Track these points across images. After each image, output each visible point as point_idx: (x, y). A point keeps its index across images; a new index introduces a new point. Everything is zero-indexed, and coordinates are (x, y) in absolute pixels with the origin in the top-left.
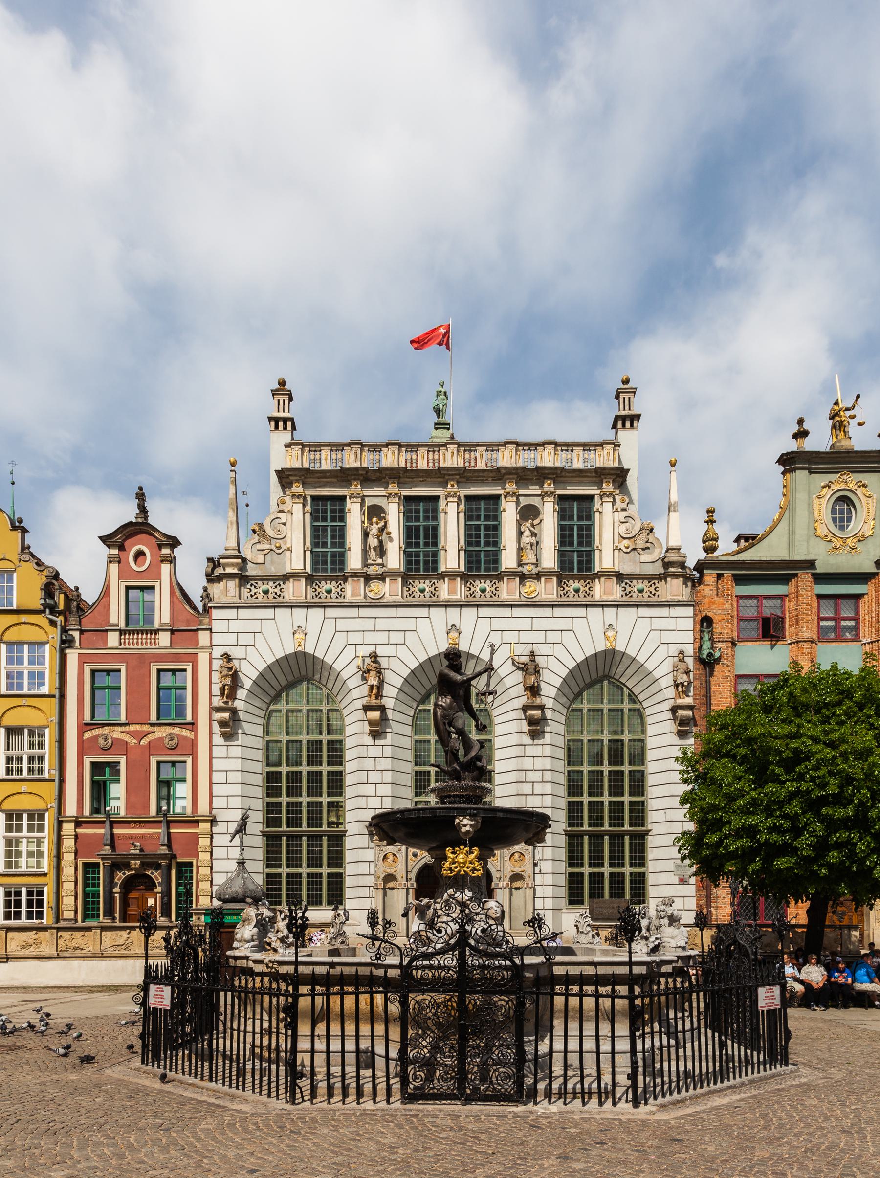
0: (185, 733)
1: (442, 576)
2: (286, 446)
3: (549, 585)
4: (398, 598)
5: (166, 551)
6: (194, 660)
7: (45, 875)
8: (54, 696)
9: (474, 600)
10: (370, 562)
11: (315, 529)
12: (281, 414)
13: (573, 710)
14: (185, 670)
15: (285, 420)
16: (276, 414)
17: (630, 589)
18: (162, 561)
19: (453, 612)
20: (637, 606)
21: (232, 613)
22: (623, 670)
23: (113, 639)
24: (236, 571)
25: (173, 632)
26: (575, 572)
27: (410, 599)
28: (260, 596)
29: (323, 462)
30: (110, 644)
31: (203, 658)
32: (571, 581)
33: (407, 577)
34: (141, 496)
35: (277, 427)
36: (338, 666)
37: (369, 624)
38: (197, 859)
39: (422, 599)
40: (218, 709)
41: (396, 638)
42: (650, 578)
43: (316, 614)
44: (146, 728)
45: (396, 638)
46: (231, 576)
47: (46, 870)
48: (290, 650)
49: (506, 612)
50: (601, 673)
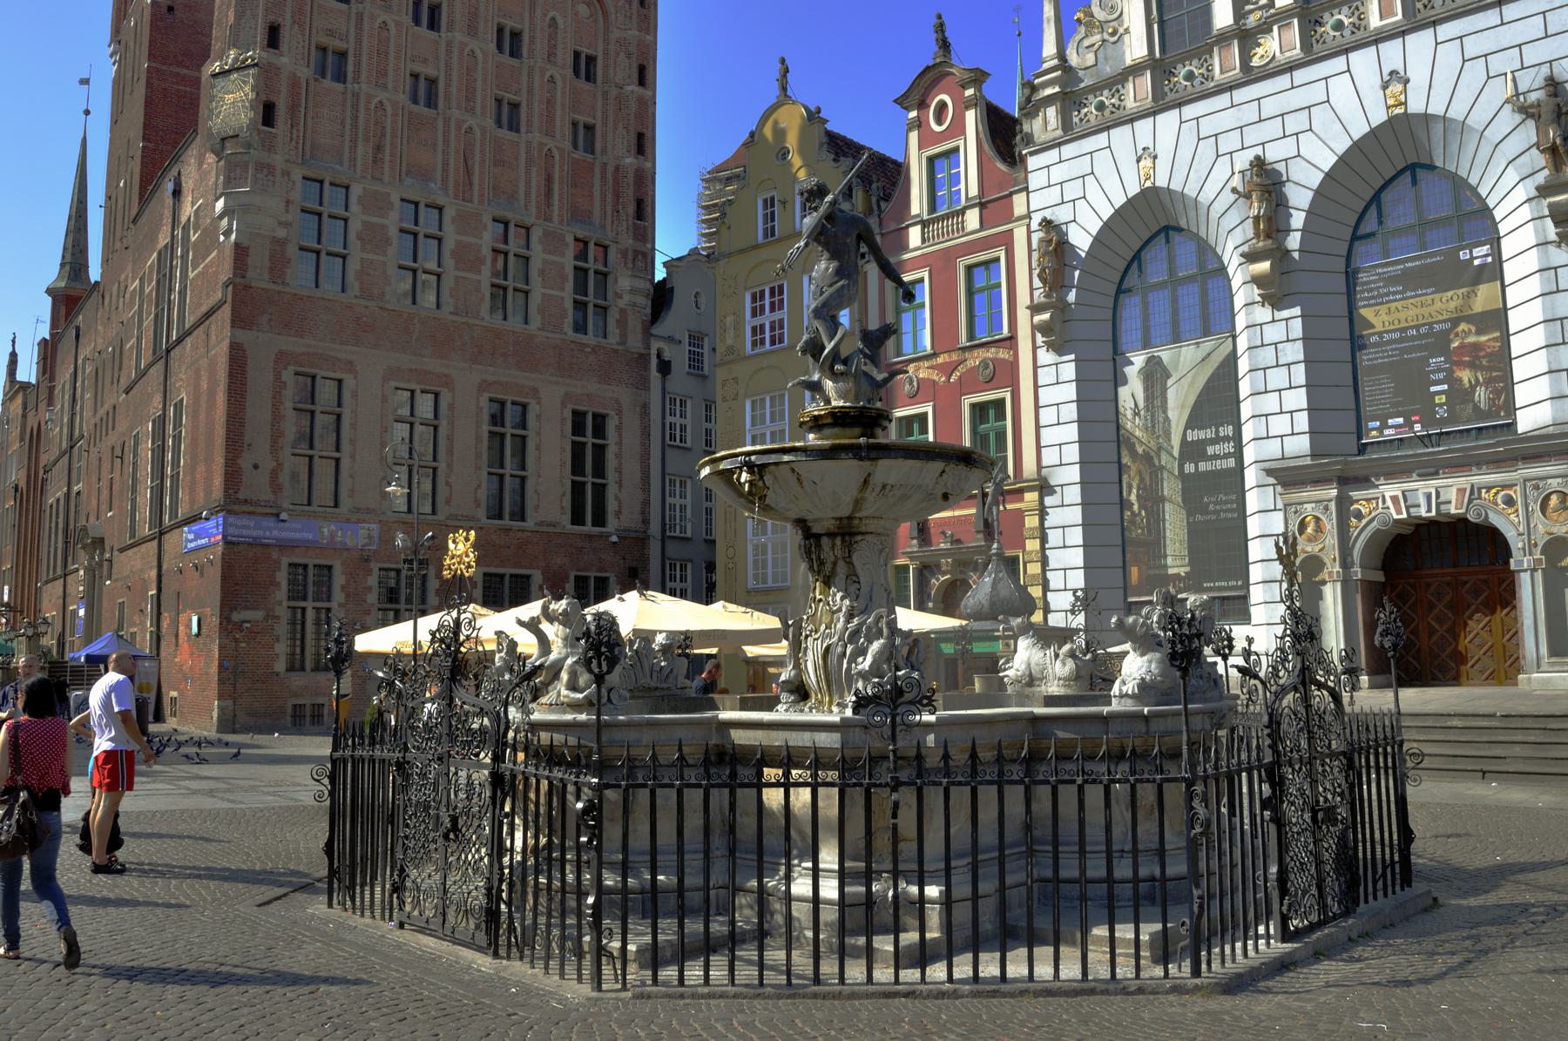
0: (1003, 354)
5: (969, 92)
6: (1007, 240)
9: (1433, 12)
10: (1248, 7)
14: (998, 259)
18: (967, 108)
19: (1391, 49)
21: (1052, 155)
24: (1057, 89)
25: (982, 206)
28: (1092, 118)
30: (912, 246)
31: (1020, 234)
34: (941, 28)
36: (1205, 198)
37: (1250, 112)
38: (1023, 547)
39: (1339, 40)
40: (1035, 309)
41: (1295, 123)
43: (1169, 119)
44: (955, 357)
45: (1295, 123)
46: (1049, 100)
48: (1134, 190)
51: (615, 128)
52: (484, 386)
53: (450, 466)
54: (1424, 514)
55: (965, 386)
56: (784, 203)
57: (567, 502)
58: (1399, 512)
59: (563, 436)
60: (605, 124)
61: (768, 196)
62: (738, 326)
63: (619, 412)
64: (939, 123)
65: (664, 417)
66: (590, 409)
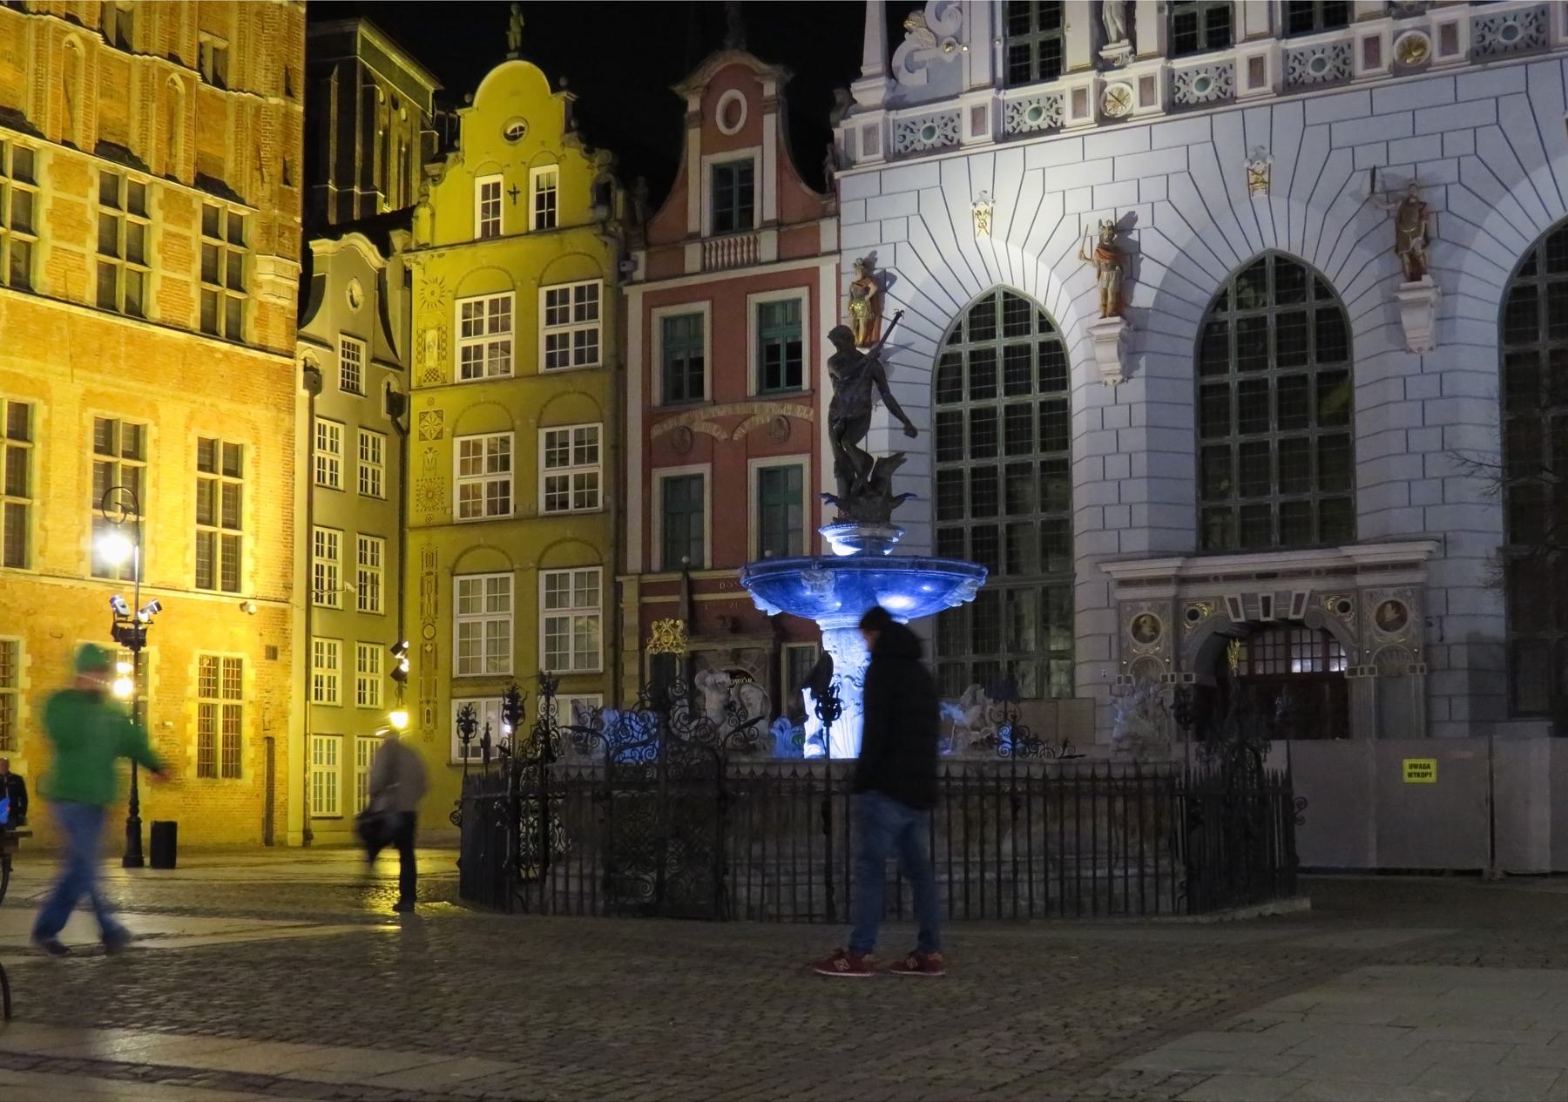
0: (801, 412)
6: (811, 280)
7: (599, 675)
30: (688, 268)
44: (741, 409)
47: (601, 669)
51: (257, 54)
52: (88, 398)
53: (44, 504)
54: (1263, 619)
55: (751, 447)
56: (514, 193)
57: (191, 558)
58: (1237, 614)
59: (186, 469)
60: (241, 48)
61: (490, 180)
62: (444, 345)
63: (257, 443)
64: (729, 122)
65: (311, 451)
66: (225, 436)
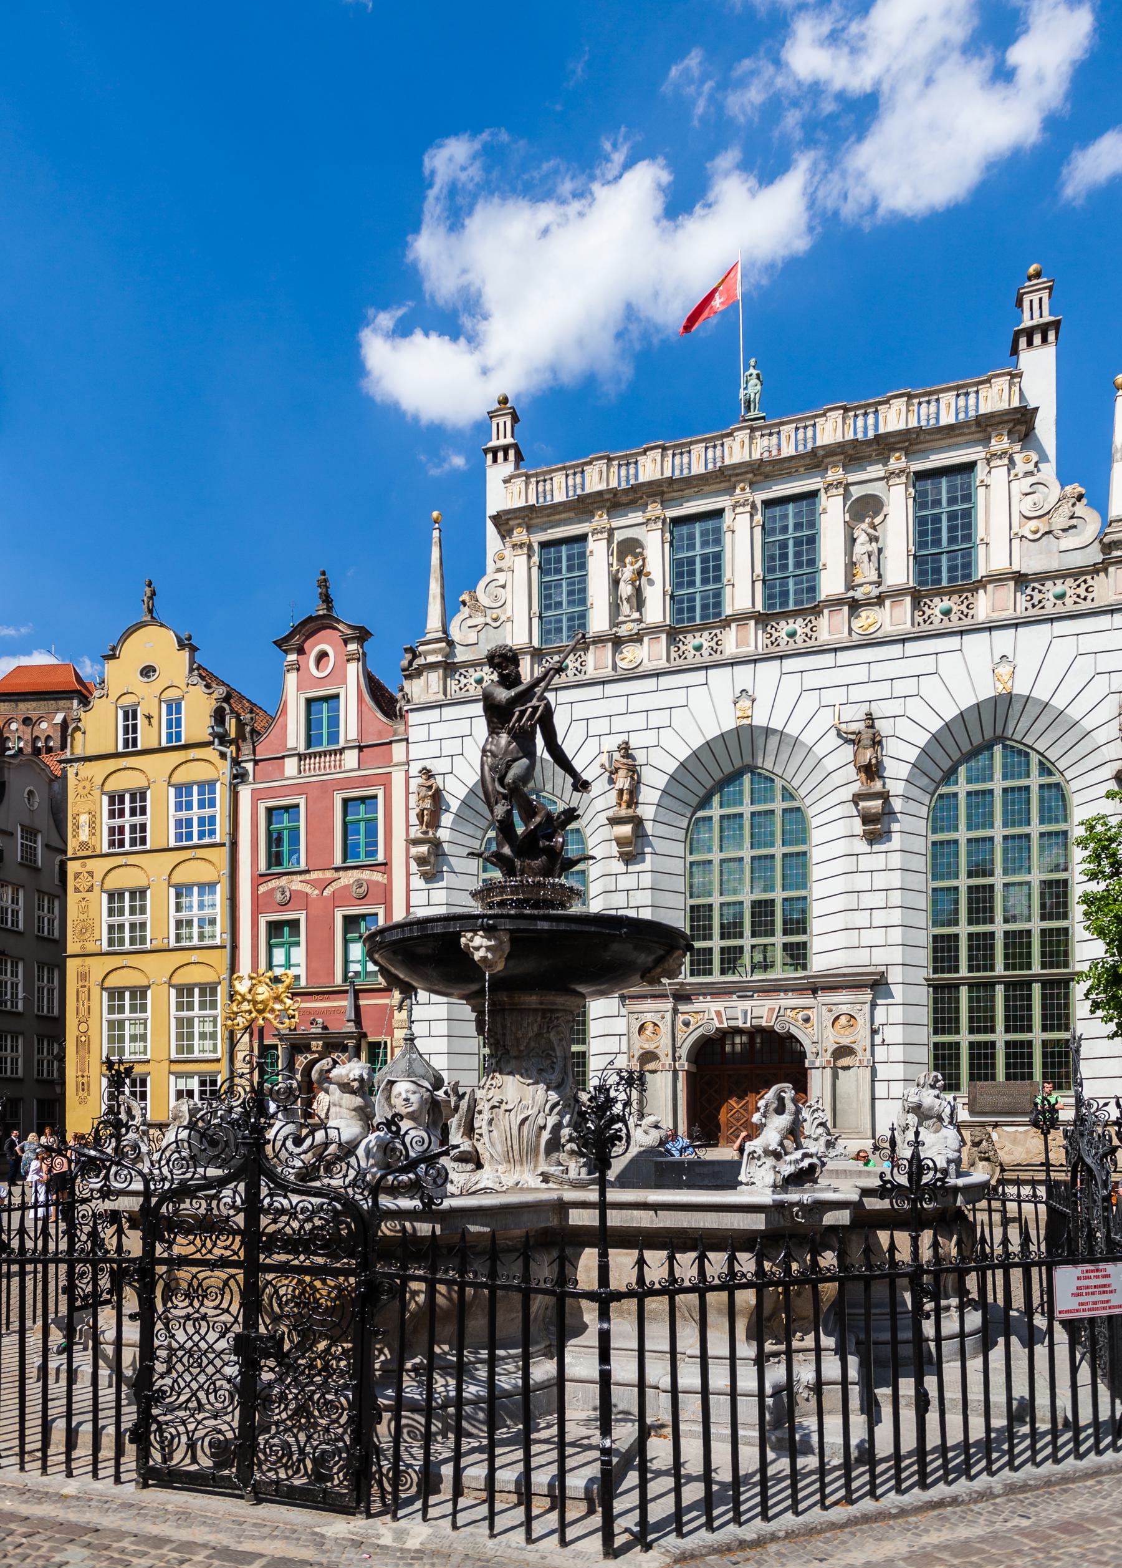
1: (726, 623)
2: (505, 482)
3: (898, 611)
4: (662, 663)
8: (223, 845)
10: (621, 619)
11: (544, 587)
12: (502, 442)
13: (941, 796)
15: (506, 449)
16: (494, 443)
17: (1041, 596)
20: (1052, 620)
22: (1028, 724)
23: (291, 766)
26: (944, 583)
27: (681, 662)
29: (556, 493)
32: (937, 600)
33: (674, 634)
35: (495, 460)
42: (1076, 574)
49: (828, 659)
50: (988, 735)
